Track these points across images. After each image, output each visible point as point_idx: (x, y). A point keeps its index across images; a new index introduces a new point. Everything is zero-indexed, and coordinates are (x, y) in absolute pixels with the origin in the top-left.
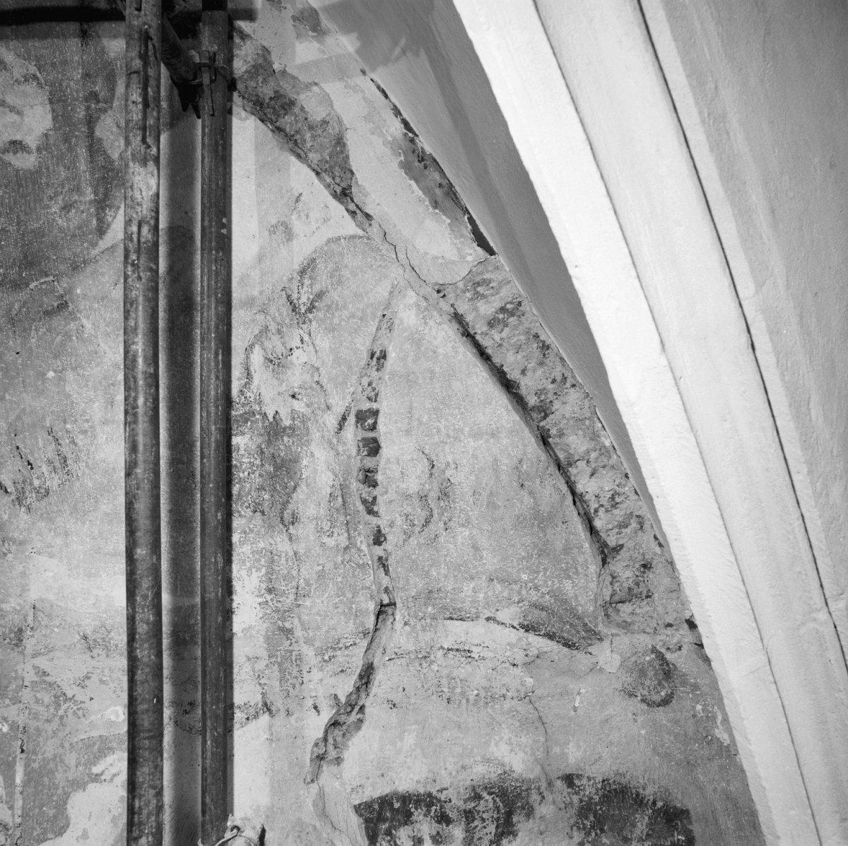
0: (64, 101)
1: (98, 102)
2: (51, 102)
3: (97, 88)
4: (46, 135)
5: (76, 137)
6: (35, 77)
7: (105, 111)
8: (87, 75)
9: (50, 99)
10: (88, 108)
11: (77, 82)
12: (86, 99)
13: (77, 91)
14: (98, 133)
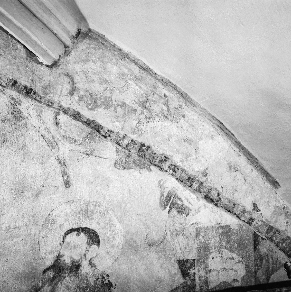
0: (249, 267)
1: (258, 266)
2: (246, 268)
3: (258, 263)
4: (243, 277)
5: (252, 277)
6: (241, 261)
7: (260, 269)
8: (255, 259)
9: (245, 267)
10: (255, 269)
11: (252, 262)
12: (255, 266)
13: (253, 264)
14: (257, 275)
